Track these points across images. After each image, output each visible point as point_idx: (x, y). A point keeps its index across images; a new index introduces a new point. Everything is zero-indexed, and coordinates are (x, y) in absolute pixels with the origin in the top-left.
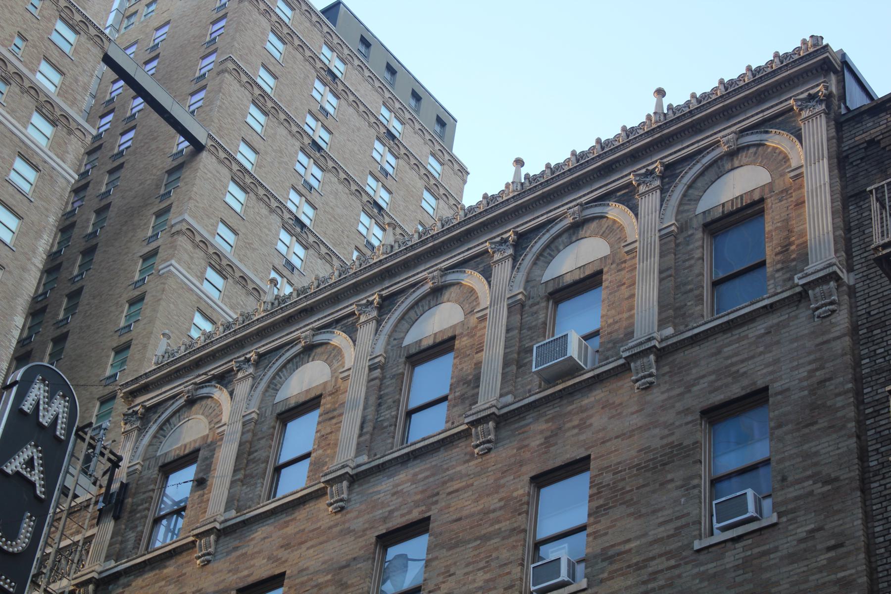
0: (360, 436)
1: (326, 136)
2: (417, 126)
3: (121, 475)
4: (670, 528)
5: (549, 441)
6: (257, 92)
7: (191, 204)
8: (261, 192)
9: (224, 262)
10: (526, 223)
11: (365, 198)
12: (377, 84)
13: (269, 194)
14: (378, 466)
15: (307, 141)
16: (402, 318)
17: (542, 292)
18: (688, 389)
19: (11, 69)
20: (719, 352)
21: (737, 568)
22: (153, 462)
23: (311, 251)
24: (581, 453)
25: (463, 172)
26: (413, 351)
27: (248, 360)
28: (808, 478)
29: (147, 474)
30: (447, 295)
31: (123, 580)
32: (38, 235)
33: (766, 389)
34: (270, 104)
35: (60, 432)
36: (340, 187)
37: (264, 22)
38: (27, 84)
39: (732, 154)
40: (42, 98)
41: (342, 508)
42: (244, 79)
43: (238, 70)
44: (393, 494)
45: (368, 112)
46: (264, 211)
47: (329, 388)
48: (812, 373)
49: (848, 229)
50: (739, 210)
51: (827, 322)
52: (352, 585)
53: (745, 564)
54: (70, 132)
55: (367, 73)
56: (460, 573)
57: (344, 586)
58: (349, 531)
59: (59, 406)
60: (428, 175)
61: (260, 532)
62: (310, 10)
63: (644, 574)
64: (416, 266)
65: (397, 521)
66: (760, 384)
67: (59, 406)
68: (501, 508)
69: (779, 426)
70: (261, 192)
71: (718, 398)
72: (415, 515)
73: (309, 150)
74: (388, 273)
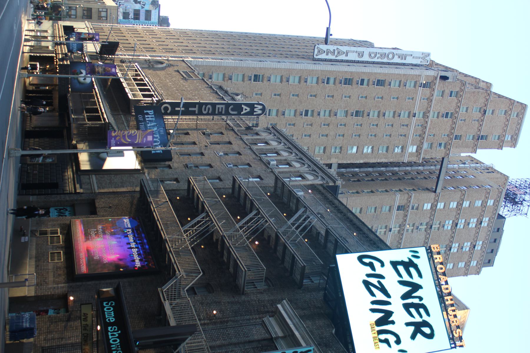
1: (462, 227)
2: (483, 254)
3: (254, 128)
6: (461, 202)
7: (418, 195)
8: (433, 213)
9: (407, 209)
10: (304, 158)
11: (450, 244)
12: (487, 237)
13: (434, 215)
15: (456, 221)
17: (289, 162)
19: (424, 136)
23: (425, 233)
25: (478, 273)
32: (386, 158)
34: (460, 207)
35: (255, 113)
36: (449, 236)
37: (483, 198)
38: (422, 141)
40: (421, 146)
42: (463, 197)
43: (464, 195)
45: (477, 237)
46: (429, 216)
54: (417, 156)
55: (489, 233)
59: (260, 112)
60: (470, 262)
61: (241, 142)
62: (496, 210)
67: (260, 112)
70: (433, 213)
73: (454, 223)
74: (295, 147)
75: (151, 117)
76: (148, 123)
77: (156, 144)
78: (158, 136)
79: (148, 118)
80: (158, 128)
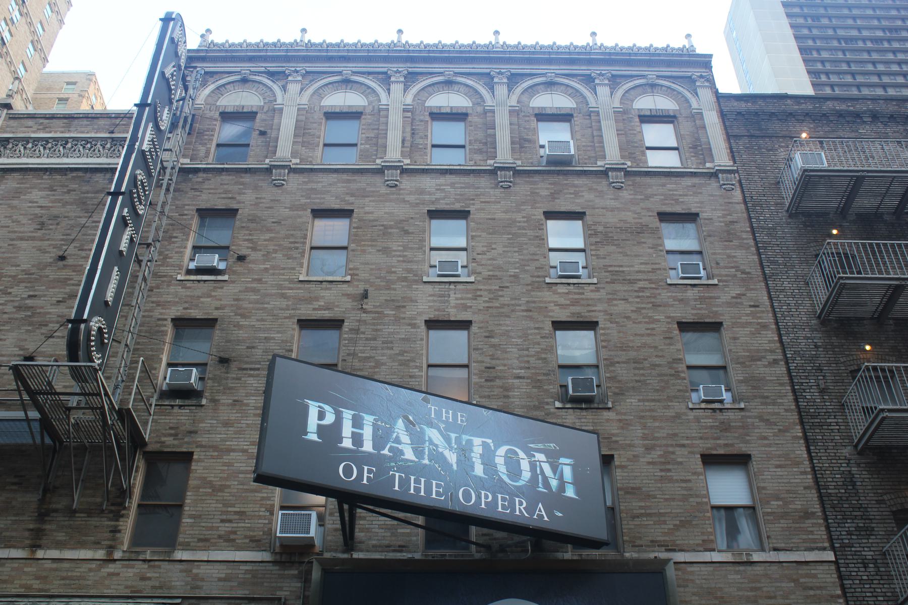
0: (403, 147)
4: (649, 268)
5: (553, 196)
16: (423, 89)
18: (647, 198)
20: (664, 185)
21: (696, 300)
22: (213, 108)
24: (578, 209)
26: (435, 111)
27: (297, 72)
28: (732, 267)
29: (209, 114)
30: (456, 87)
31: (201, 174)
33: (697, 215)
39: (653, 86)
41: (396, 185)
44: (437, 190)
47: (368, 110)
48: (724, 216)
49: (732, 152)
50: (659, 116)
51: (729, 193)
52: (412, 233)
53: (702, 299)
56: (500, 249)
57: (407, 232)
58: (404, 201)
61: (326, 180)
63: (636, 287)
65: (442, 206)
66: (694, 210)
68: (524, 222)
69: (710, 236)
71: (668, 209)
72: (457, 206)
75: (357, 423)
76: (397, 452)
77: (525, 465)
78: (477, 441)
79: (357, 439)
80: (431, 425)
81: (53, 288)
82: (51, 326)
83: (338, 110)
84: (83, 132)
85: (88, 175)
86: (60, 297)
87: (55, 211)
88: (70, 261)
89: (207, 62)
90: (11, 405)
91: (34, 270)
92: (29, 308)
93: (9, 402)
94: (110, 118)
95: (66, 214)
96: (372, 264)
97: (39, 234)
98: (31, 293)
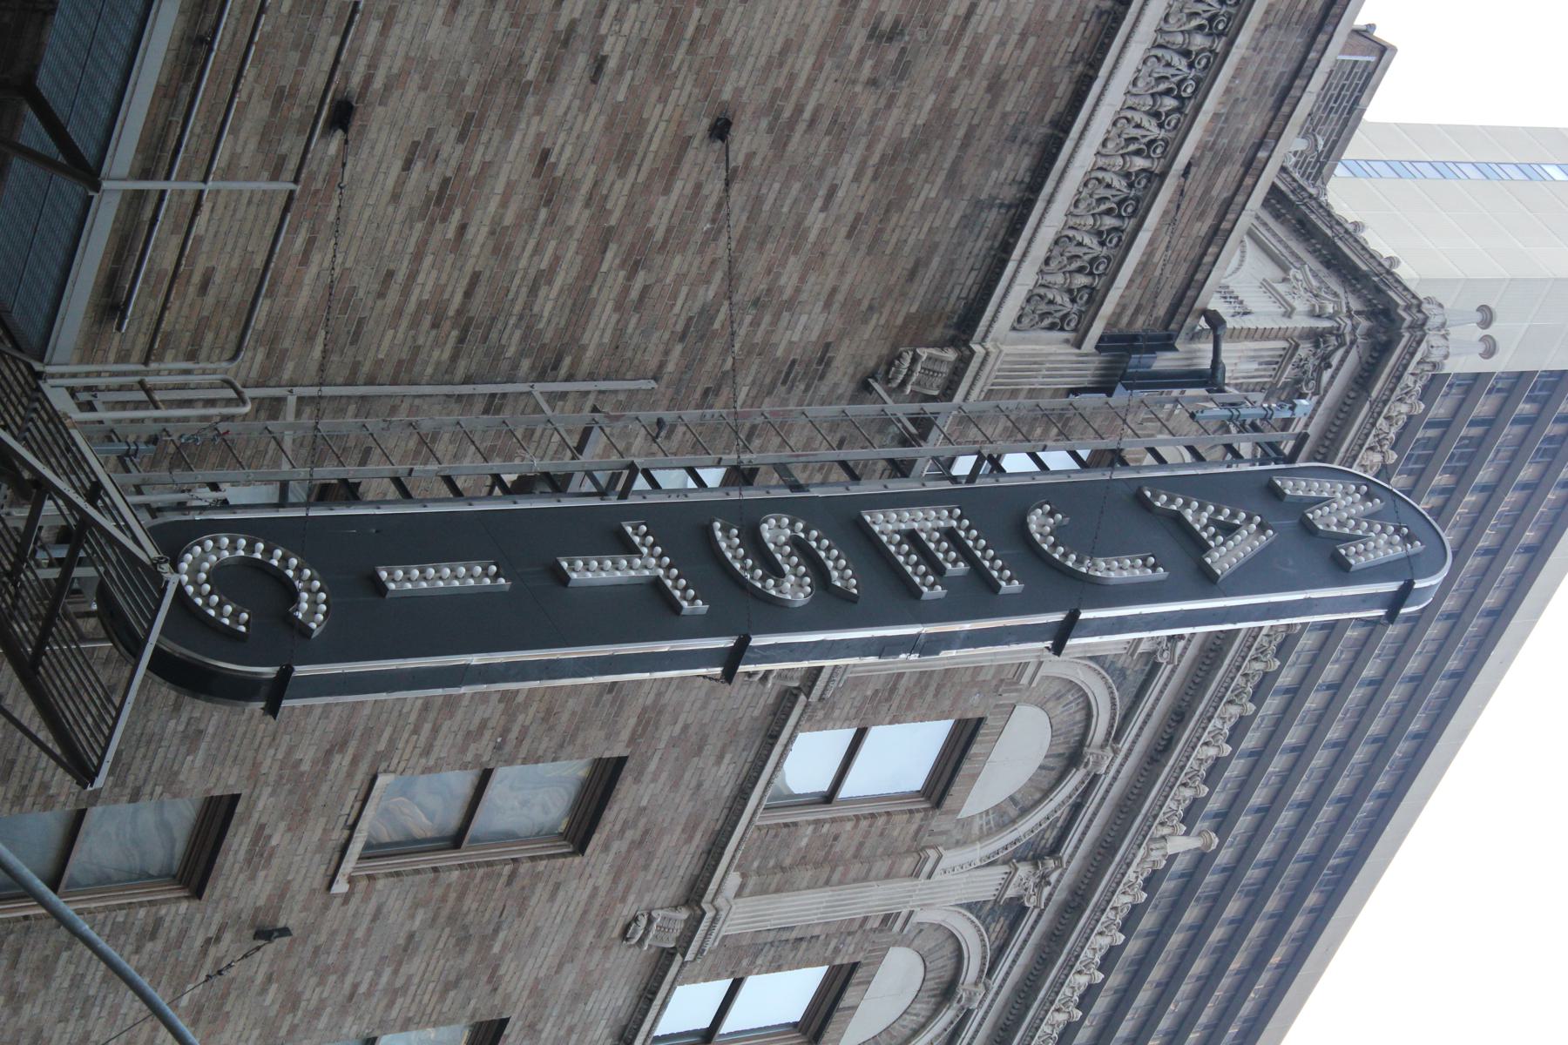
14: (655, 993)
30: (923, 1009)
64: (1039, 948)
81: (610, 126)
82: (451, 151)
83: (975, 749)
84: (1238, 72)
85: (1041, 131)
86: (562, 157)
87: (928, 67)
88: (702, 155)
89: (1348, 388)
90: (175, 97)
91: (708, 49)
92: (550, 72)
93: (186, 92)
94: (1259, 146)
95: (902, 100)
96: (369, 931)
97: (857, 36)
98: (612, 64)
